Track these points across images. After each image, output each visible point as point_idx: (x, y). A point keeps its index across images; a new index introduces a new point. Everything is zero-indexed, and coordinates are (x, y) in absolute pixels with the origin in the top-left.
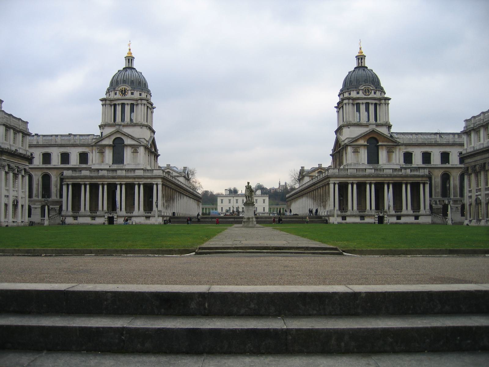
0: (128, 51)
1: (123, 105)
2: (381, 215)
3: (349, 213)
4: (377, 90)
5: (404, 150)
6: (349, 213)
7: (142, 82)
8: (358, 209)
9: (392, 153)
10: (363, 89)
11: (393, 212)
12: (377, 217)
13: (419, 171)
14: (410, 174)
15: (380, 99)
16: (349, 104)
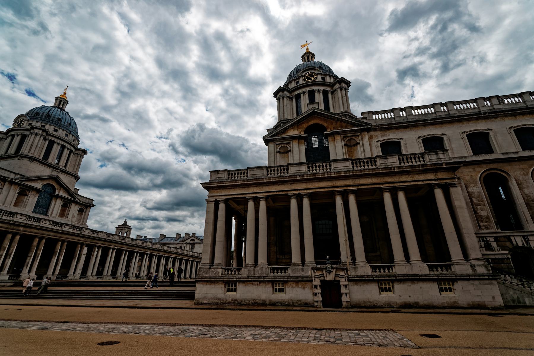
0: (62, 94)
1: (13, 136)
2: (330, 277)
3: (244, 273)
4: (326, 75)
5: (380, 137)
6: (244, 273)
7: (52, 116)
8: (269, 263)
9: (355, 148)
10: (304, 75)
11: (366, 270)
12: (320, 283)
13: (423, 158)
14: (400, 166)
15: (332, 85)
16: (283, 98)
